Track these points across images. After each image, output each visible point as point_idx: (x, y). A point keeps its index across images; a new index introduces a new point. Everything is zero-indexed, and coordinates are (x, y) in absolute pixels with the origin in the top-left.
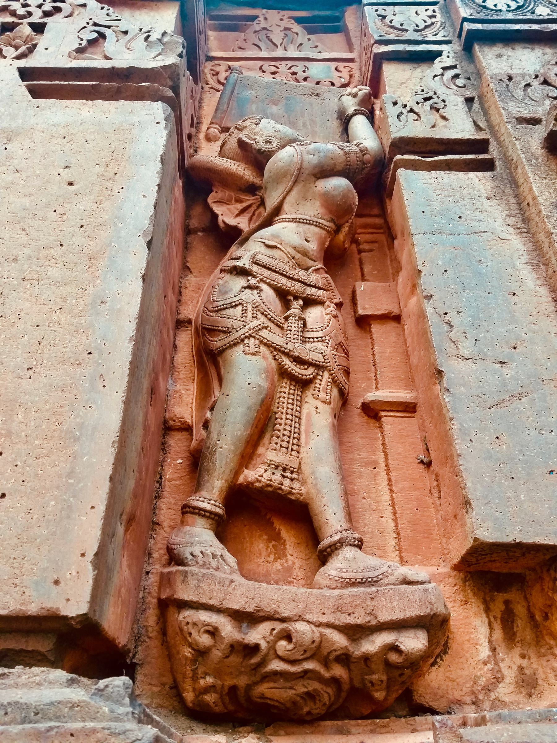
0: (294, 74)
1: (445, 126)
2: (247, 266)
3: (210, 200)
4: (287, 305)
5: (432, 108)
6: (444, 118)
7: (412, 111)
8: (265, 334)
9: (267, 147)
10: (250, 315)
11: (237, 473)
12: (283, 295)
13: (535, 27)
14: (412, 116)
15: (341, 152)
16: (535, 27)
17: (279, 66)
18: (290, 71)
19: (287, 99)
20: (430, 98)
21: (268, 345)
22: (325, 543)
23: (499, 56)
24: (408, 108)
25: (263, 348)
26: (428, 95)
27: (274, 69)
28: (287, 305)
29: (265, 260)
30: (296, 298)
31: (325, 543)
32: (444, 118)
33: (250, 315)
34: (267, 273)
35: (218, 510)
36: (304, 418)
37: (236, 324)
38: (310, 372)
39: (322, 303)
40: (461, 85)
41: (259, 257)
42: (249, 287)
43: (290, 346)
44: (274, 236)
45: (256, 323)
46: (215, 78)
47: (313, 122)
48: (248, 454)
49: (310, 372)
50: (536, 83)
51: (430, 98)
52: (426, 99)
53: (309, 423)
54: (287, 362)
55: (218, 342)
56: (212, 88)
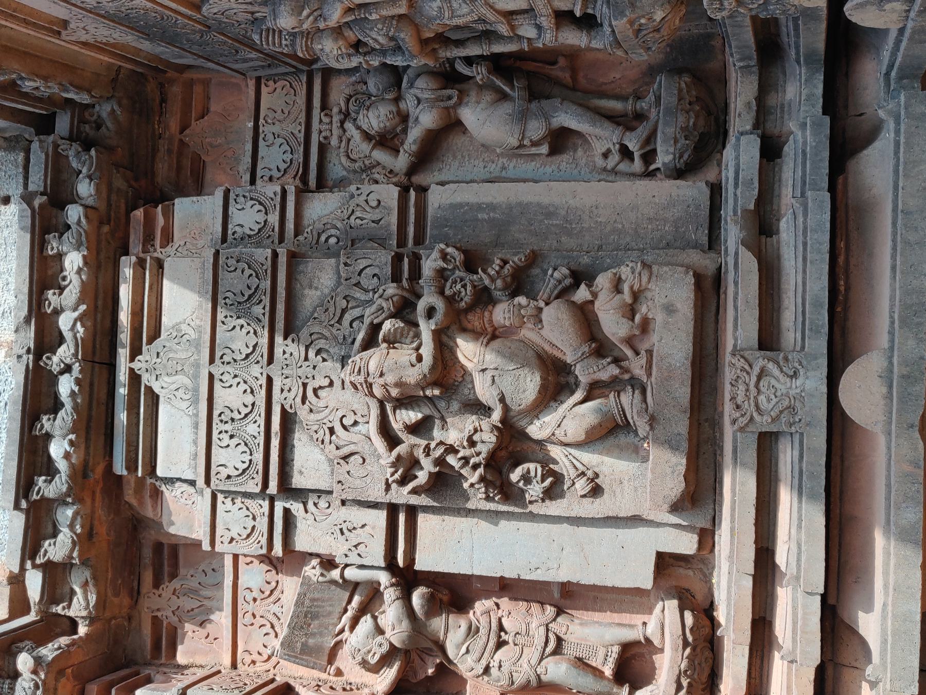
0: (255, 600)
1: (373, 528)
2: (484, 667)
3: (415, 681)
4: (505, 643)
5: (350, 531)
6: (363, 526)
7: (356, 546)
8: (534, 661)
9: (385, 648)
10: (519, 669)
11: (608, 679)
12: (500, 644)
13: (275, 443)
14: (361, 548)
15: (397, 602)
16: (275, 443)
17: (244, 611)
18: (252, 602)
19: (306, 616)
20: (341, 530)
21: (541, 659)
22: (643, 641)
23: (301, 473)
24: (353, 549)
25: (542, 664)
26: (339, 532)
27: (249, 615)
28: (505, 643)
29: (477, 655)
30: (500, 637)
31: (643, 641)
32: (363, 526)
33: (519, 669)
34: (486, 655)
35: (627, 689)
36: (577, 641)
37: (526, 676)
38: (552, 638)
39: (500, 619)
40: (327, 505)
41: (474, 658)
42: (500, 666)
43: (539, 648)
44: (459, 647)
45: (525, 666)
46: (257, 664)
47: (330, 599)
48: (597, 673)
49: (552, 638)
50: (346, 467)
51: (341, 530)
52: (342, 533)
53: (582, 639)
54: (549, 649)
55: (534, 683)
56: (274, 668)
